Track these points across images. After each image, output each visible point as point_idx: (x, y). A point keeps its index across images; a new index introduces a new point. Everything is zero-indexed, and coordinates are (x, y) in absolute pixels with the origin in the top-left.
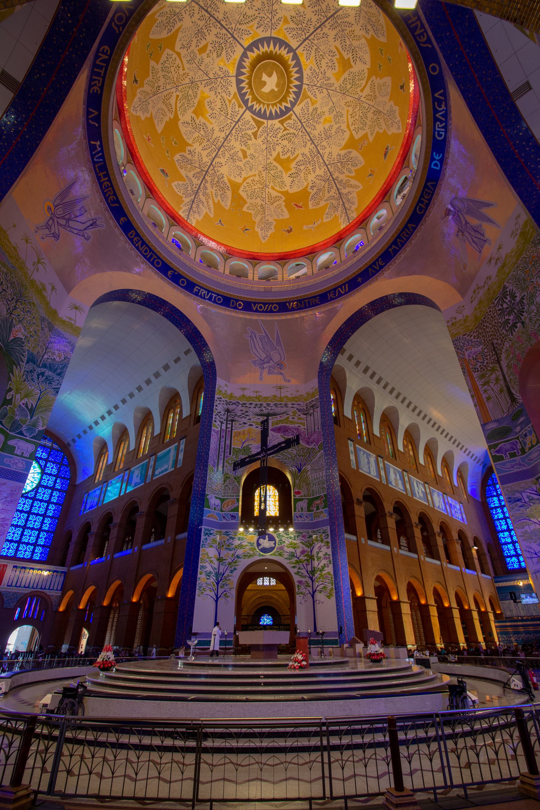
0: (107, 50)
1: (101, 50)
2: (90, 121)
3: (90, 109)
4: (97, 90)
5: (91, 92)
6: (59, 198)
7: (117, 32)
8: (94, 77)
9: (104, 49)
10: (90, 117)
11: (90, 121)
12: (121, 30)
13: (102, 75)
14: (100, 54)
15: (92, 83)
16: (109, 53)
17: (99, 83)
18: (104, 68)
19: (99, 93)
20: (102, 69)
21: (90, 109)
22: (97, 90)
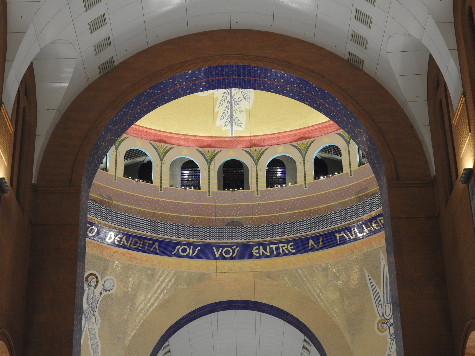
0: (256, 250)
1: (258, 255)
2: (320, 246)
3: (310, 248)
4: (291, 246)
5: (294, 251)
6: (377, 305)
7: (238, 249)
8: (281, 252)
9: (256, 253)
10: (316, 247)
11: (320, 246)
12: (235, 247)
13: (277, 246)
14: (261, 255)
15: (287, 252)
16: (257, 247)
17: (285, 246)
18: (271, 246)
19: (292, 243)
20: (272, 248)
21: (310, 248)
22: (291, 246)
